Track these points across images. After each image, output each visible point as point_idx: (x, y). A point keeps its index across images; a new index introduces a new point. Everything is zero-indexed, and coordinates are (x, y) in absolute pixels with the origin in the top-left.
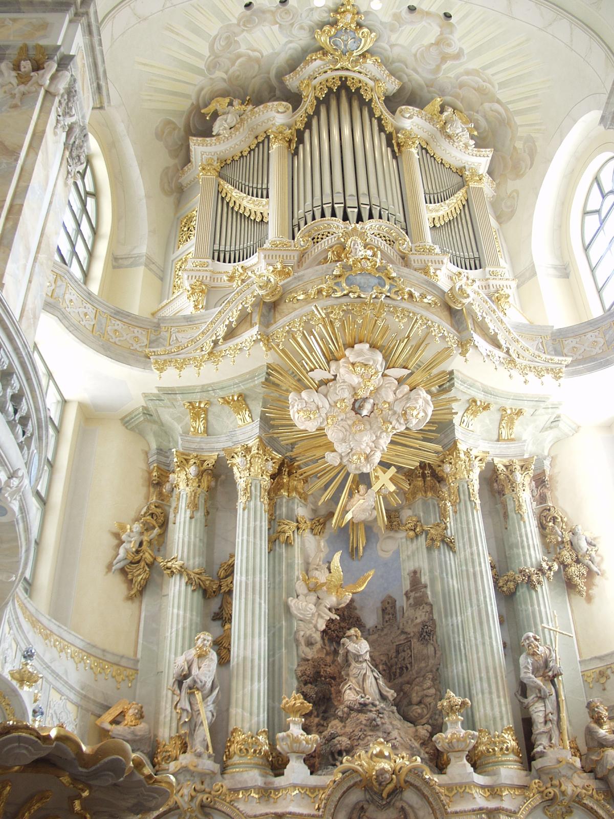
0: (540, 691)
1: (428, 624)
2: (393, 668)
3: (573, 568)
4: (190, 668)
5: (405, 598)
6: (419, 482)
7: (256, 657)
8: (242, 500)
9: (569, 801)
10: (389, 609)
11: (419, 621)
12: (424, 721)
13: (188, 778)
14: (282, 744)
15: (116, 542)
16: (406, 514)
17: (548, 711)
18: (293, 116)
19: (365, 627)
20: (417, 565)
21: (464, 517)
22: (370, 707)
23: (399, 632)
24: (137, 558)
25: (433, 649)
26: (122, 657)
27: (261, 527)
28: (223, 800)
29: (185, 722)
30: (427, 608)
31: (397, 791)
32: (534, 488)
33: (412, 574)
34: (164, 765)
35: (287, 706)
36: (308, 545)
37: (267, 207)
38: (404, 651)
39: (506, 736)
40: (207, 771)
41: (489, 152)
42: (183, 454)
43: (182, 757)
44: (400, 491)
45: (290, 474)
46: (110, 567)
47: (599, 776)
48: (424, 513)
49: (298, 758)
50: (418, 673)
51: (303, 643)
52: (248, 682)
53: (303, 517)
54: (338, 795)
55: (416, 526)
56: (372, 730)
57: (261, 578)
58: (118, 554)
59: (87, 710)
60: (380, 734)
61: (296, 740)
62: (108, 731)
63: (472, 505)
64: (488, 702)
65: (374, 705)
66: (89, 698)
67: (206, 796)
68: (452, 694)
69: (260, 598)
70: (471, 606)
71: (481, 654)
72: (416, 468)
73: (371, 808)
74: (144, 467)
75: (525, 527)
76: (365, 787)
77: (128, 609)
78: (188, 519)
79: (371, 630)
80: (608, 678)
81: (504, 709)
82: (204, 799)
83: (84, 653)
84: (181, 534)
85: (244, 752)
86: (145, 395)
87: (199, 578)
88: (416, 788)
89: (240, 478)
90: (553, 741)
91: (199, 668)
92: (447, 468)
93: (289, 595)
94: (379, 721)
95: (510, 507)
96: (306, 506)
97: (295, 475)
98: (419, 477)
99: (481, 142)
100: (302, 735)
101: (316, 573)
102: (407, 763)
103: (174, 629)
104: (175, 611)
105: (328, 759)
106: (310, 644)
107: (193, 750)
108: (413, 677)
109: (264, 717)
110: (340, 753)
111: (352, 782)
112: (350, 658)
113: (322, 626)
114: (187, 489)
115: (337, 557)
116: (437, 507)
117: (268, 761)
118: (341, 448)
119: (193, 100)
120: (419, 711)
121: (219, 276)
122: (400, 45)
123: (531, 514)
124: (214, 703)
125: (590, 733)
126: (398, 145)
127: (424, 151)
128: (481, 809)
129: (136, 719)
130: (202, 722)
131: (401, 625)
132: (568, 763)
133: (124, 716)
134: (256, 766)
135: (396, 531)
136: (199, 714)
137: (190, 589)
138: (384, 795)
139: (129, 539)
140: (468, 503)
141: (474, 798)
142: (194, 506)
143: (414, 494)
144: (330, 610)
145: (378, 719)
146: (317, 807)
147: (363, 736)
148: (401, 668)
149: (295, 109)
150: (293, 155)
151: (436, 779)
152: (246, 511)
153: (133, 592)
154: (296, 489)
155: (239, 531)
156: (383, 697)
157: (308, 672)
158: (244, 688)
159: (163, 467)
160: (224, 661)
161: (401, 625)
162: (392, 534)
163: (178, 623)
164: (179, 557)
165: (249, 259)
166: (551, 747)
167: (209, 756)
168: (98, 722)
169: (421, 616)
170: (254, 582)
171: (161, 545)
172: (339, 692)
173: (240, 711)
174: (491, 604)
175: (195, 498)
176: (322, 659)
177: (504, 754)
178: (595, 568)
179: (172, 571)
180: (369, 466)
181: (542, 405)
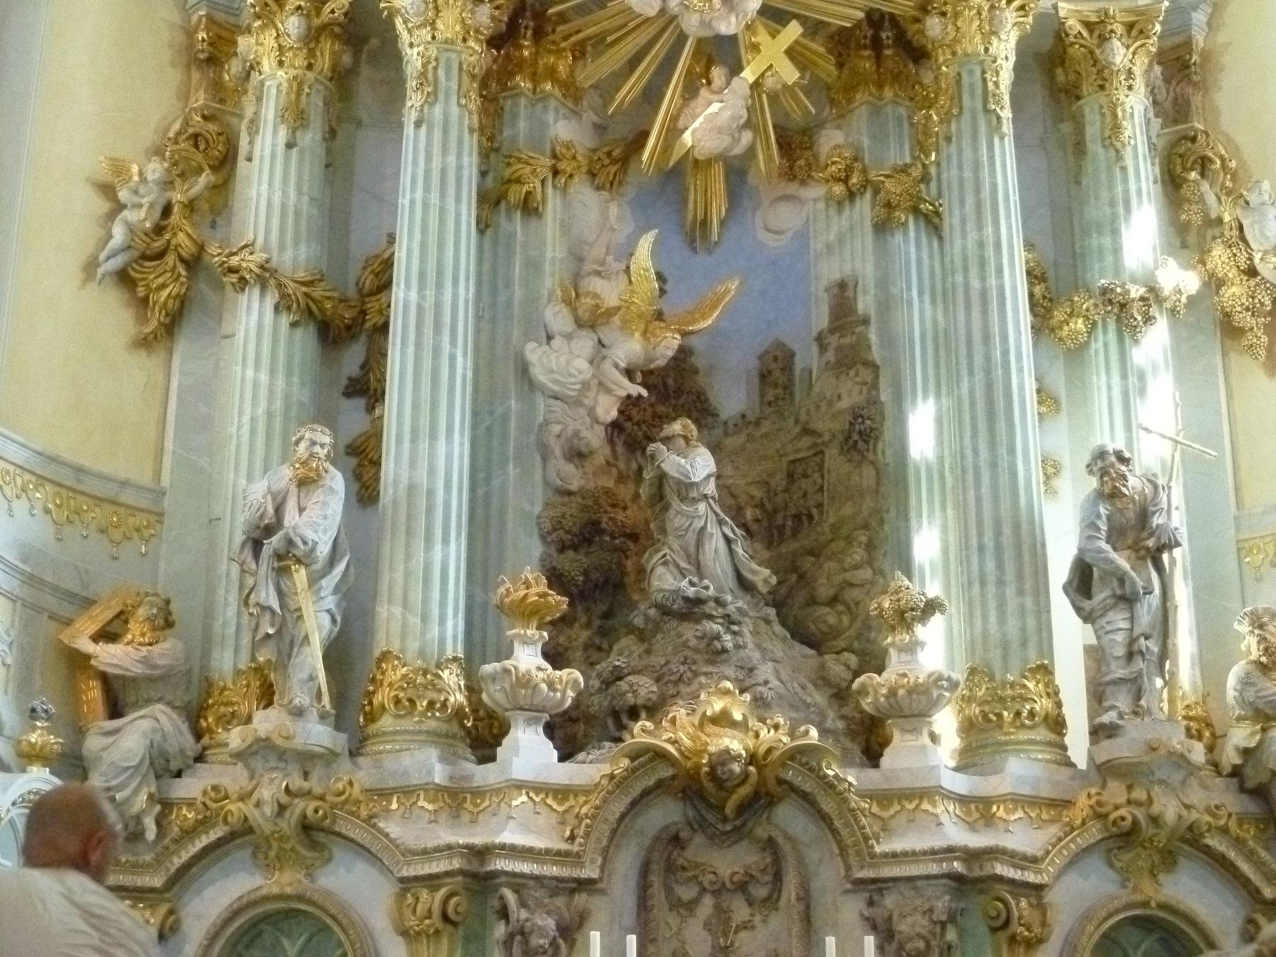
0: (1122, 581)
1: (865, 412)
5: (815, 348)
7: (440, 485)
8: (414, 100)
9: (1169, 841)
10: (777, 373)
11: (844, 404)
12: (840, 643)
13: (273, 763)
14: (492, 688)
15: (103, 206)
16: (830, 140)
17: (1137, 631)
19: (717, 415)
20: (847, 269)
21: (968, 154)
22: (710, 608)
23: (797, 429)
24: (158, 244)
25: (873, 473)
26: (125, 484)
27: (459, 168)
28: (352, 814)
29: (268, 636)
30: (866, 374)
32: (1159, 82)
33: (836, 291)
34: (221, 734)
35: (507, 600)
36: (579, 214)
38: (805, 476)
39: (1031, 685)
40: (317, 749)
43: (259, 716)
44: (814, 87)
45: (539, 34)
46: (90, 267)
47: (1250, 784)
48: (873, 137)
49: (530, 722)
50: (835, 528)
51: (558, 453)
52: (419, 543)
53: (568, 146)
54: (619, 807)
55: (849, 170)
56: (712, 662)
57: (455, 295)
58: (111, 237)
60: (730, 671)
61: (525, 682)
62: (88, 657)
63: (989, 122)
64: (992, 604)
65: (719, 602)
66: (42, 582)
69: (453, 342)
70: (971, 373)
71: (985, 490)
72: (858, 25)
73: (699, 839)
74: (176, 17)
75: (1125, 180)
76: (684, 791)
77: (138, 371)
78: (281, 148)
79: (731, 424)
82: (310, 813)
83: (27, 477)
84: (265, 187)
85: (405, 706)
87: (306, 295)
88: (806, 797)
89: (411, 45)
90: (1143, 702)
91: (301, 510)
93: (528, 336)
95: (1092, 129)
96: (576, 114)
97: (551, 37)
98: (865, 47)
100: (539, 669)
101: (597, 285)
102: (785, 739)
103: (246, 419)
104: (250, 373)
105: (605, 727)
106: (578, 455)
107: (286, 701)
108: (822, 538)
109: (455, 627)
110: (634, 713)
111: (651, 782)
112: (667, 491)
113: (608, 410)
114: (281, 73)
115: (646, 243)
116: (906, 125)
117: (463, 726)
120: (832, 620)
123: (1142, 149)
124: (336, 590)
128: (950, 850)
129: (154, 629)
130: (306, 637)
131: (803, 410)
132: (1171, 754)
133: (126, 622)
134: (435, 738)
135: (803, 183)
136: (300, 617)
137: (285, 320)
138: (729, 808)
139: (136, 199)
141: (940, 824)
142: (296, 117)
143: (850, 90)
144: (629, 373)
145: (728, 637)
146: (568, 833)
147: (689, 674)
148: (797, 517)
151: (850, 779)
152: (424, 129)
153: (147, 330)
154: (552, 74)
155: (405, 179)
156: (744, 584)
157: (568, 523)
158: (408, 556)
159: (220, 16)
160: (365, 491)
161: (803, 410)
162: (793, 188)
163: (255, 404)
164: (260, 241)
166: (1136, 713)
167: (323, 717)
169: (849, 394)
170: (438, 306)
171: (219, 214)
172: (642, 572)
173: (397, 610)
174: (1020, 370)
175: (299, 95)
176: (608, 492)
177: (1023, 726)
179: (242, 279)
180: (733, 19)
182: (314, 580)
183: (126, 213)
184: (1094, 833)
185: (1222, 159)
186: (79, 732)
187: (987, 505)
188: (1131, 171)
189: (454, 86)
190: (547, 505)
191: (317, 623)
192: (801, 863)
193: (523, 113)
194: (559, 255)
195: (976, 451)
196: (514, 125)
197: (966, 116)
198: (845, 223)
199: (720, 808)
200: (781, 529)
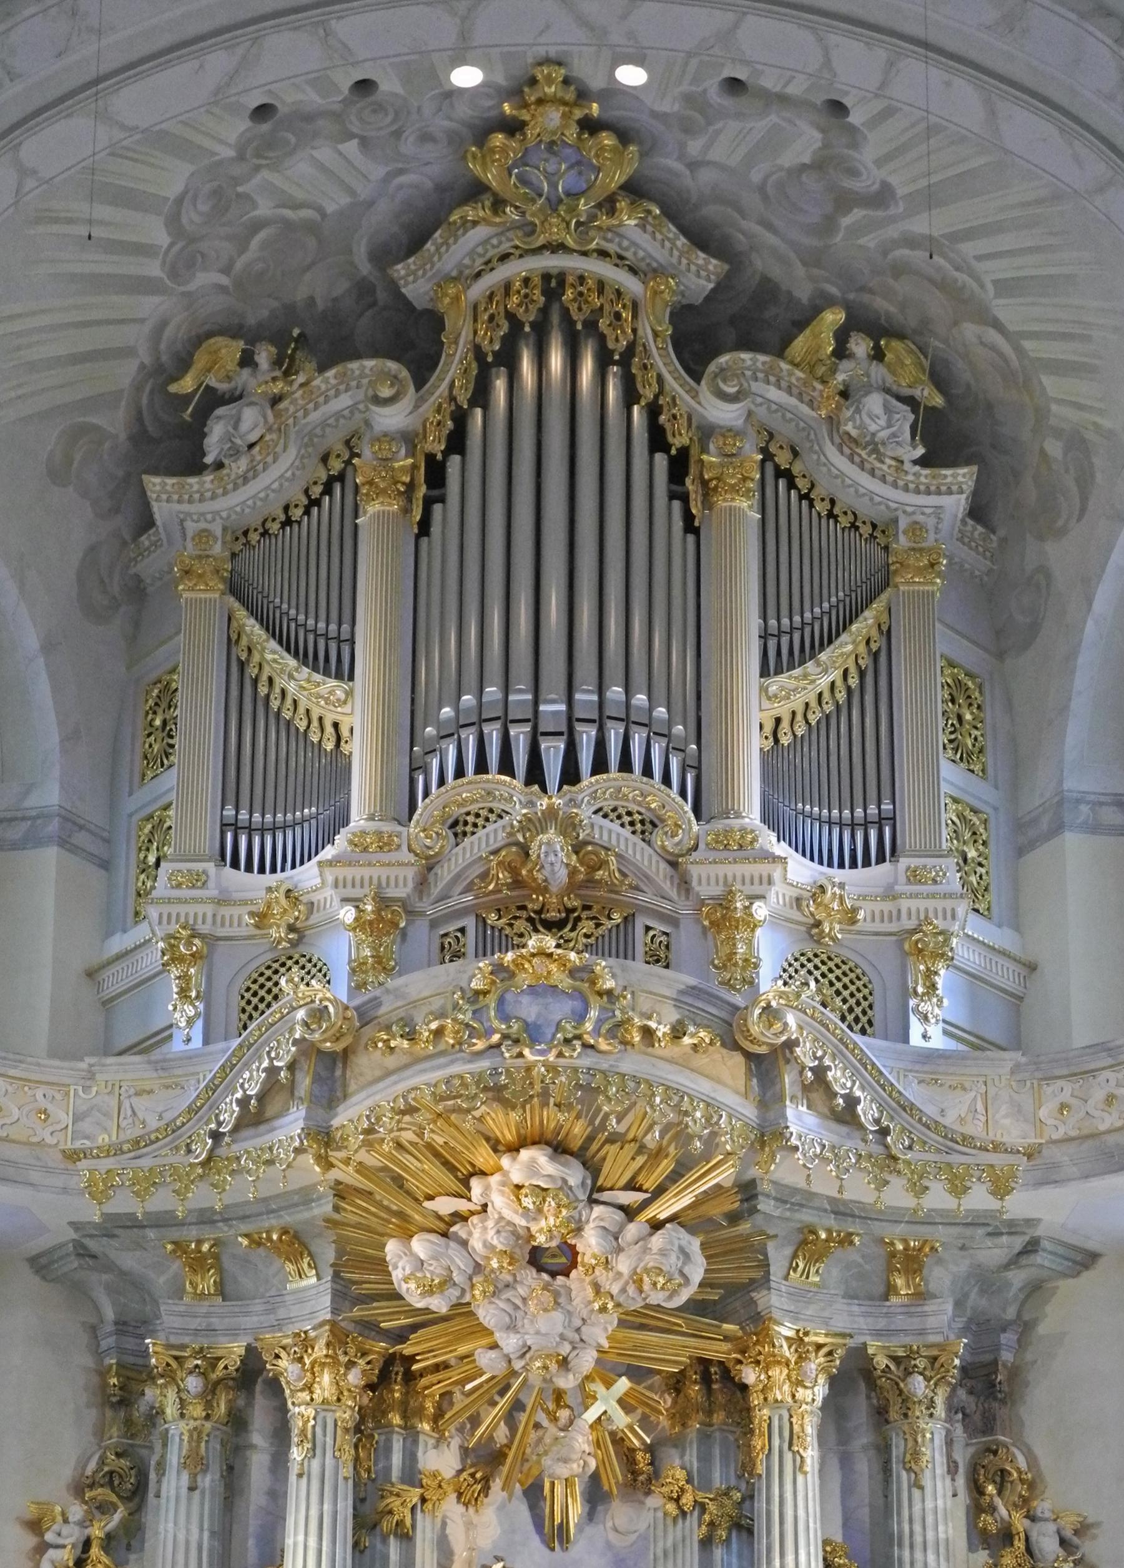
37: (347, 709)
41: (964, 476)
86: (76, 1226)
92: (750, 1375)
99: (943, 439)
121: (236, 911)
122: (714, 164)
126: (705, 483)
127: (782, 483)
149: (420, 382)
150: (418, 537)
152: (304, 1480)
183: (51, 1553)
189: (329, 1440)
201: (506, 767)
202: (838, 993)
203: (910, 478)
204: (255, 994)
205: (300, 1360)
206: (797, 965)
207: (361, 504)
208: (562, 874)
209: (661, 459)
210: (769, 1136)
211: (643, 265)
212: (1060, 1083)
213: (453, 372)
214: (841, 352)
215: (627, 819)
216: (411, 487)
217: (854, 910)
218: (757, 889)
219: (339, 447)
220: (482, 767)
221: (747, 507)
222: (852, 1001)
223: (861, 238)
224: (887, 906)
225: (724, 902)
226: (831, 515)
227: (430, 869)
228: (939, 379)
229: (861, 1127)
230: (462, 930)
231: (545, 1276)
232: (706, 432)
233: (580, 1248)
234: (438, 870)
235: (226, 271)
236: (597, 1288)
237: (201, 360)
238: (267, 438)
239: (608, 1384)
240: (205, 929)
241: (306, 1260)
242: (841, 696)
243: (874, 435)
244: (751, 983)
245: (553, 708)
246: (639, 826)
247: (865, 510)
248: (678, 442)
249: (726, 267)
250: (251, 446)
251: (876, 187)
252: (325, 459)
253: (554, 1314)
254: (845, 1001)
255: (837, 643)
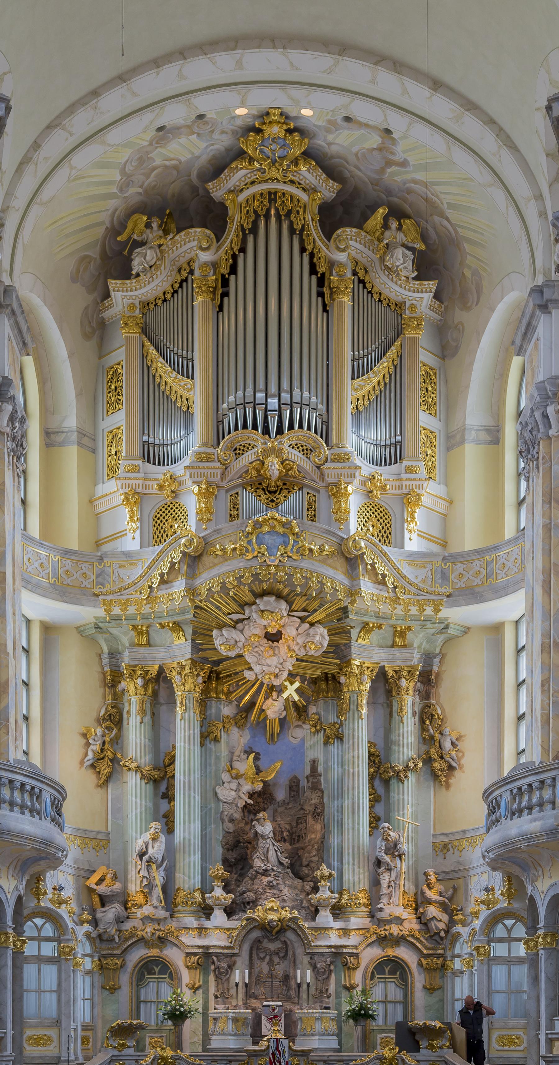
2: (292, 837)
3: (436, 764)
4: (147, 847)
6: (323, 685)
8: (179, 710)
12: (309, 879)
18: (217, 251)
21: (351, 725)
24: (102, 756)
27: (194, 734)
30: (319, 794)
31: (282, 930)
37: (192, 393)
41: (432, 285)
42: (131, 666)
49: (219, 909)
50: (309, 842)
51: (226, 820)
53: (227, 717)
56: (270, 889)
59: (79, 876)
61: (218, 899)
62: (95, 890)
64: (351, 871)
65: (273, 870)
67: (161, 933)
68: (325, 867)
69: (194, 793)
73: (266, 940)
78: (138, 724)
80: (448, 850)
81: (362, 876)
83: (73, 837)
84: (134, 737)
86: (96, 618)
88: (295, 930)
92: (343, 679)
94: (275, 883)
106: (232, 820)
113: (241, 804)
118: (257, 669)
119: (108, 224)
120: (306, 872)
125: (423, 893)
126: (331, 289)
127: (361, 285)
137: (143, 782)
138: (274, 933)
140: (356, 713)
148: (299, 836)
150: (218, 312)
152: (183, 721)
157: (230, 843)
158: (184, 860)
162: (300, 723)
165: (177, 464)
167: (163, 907)
168: (87, 883)
173: (181, 875)
178: (454, 764)
181: (428, 623)
182: (158, 867)
183: (91, 746)
184: (374, 938)
185: (438, 715)
186: (93, 911)
187: (351, 840)
188: (405, 724)
190: (224, 837)
191: (159, 879)
192: (293, 947)
193: (213, 705)
194: (226, 754)
195: (348, 824)
196: (211, 710)
197: (351, 712)
198: (316, 740)
199: (271, 932)
200: (294, 839)
201: (255, 427)
202: (378, 520)
203: (411, 285)
204: (159, 519)
205: (180, 674)
206: (363, 509)
207: (195, 296)
208: (277, 473)
209: (314, 278)
210: (353, 592)
211: (308, 187)
212: (459, 565)
213: (232, 235)
214: (386, 226)
215: (301, 449)
216: (215, 288)
217: (385, 486)
218: (349, 480)
219: (185, 265)
220: (245, 427)
221: (347, 300)
222: (383, 524)
223: (395, 177)
224: (397, 483)
225: (337, 484)
226: (380, 300)
227: (226, 468)
228: (424, 238)
229: (387, 586)
230: (237, 493)
231: (270, 642)
232: (331, 264)
233: (283, 632)
234: (229, 469)
235: (141, 187)
236: (289, 647)
237: (130, 225)
238: (158, 263)
239: (292, 683)
240: (140, 490)
241: (181, 633)
242: (382, 387)
243: (398, 267)
244: (347, 520)
245: (273, 402)
246: (305, 452)
247: (393, 296)
248: (321, 270)
249: (341, 186)
250: (151, 267)
251: (402, 159)
252: (179, 271)
253: (273, 658)
254: (381, 524)
255: (381, 362)
